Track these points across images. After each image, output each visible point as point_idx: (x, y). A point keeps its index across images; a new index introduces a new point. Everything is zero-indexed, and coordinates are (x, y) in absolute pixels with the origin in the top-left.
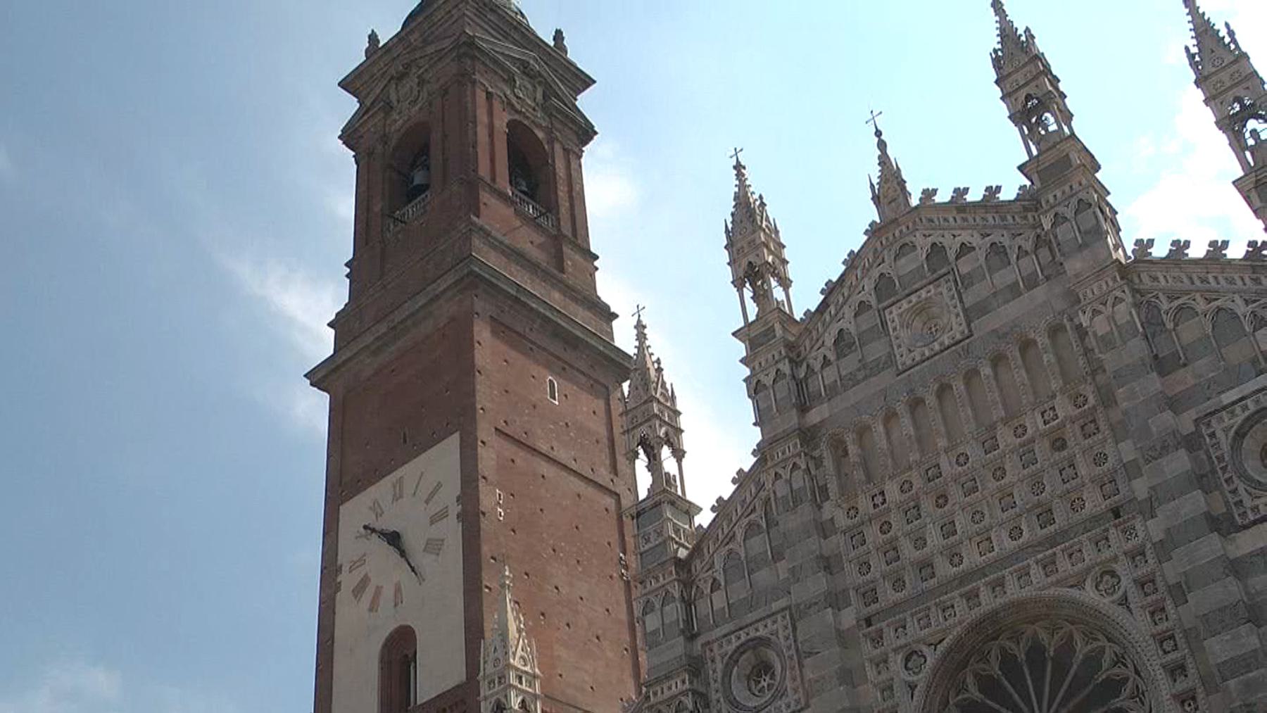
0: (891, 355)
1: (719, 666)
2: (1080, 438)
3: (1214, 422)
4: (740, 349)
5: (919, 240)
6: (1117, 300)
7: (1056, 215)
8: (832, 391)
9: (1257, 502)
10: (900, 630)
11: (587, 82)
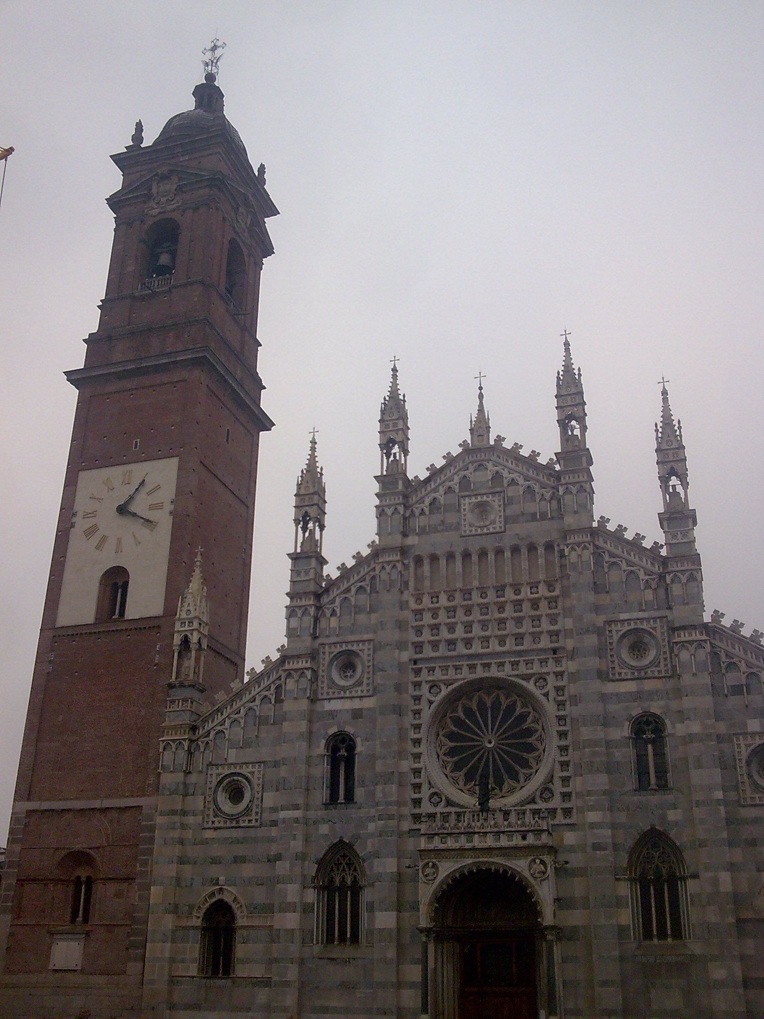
0: (459, 524)
1: (327, 659)
2: (547, 607)
3: (613, 626)
4: (376, 487)
5: (490, 466)
6: (585, 548)
7: (567, 488)
8: (423, 532)
9: (623, 671)
10: (431, 672)
11: (275, 212)
